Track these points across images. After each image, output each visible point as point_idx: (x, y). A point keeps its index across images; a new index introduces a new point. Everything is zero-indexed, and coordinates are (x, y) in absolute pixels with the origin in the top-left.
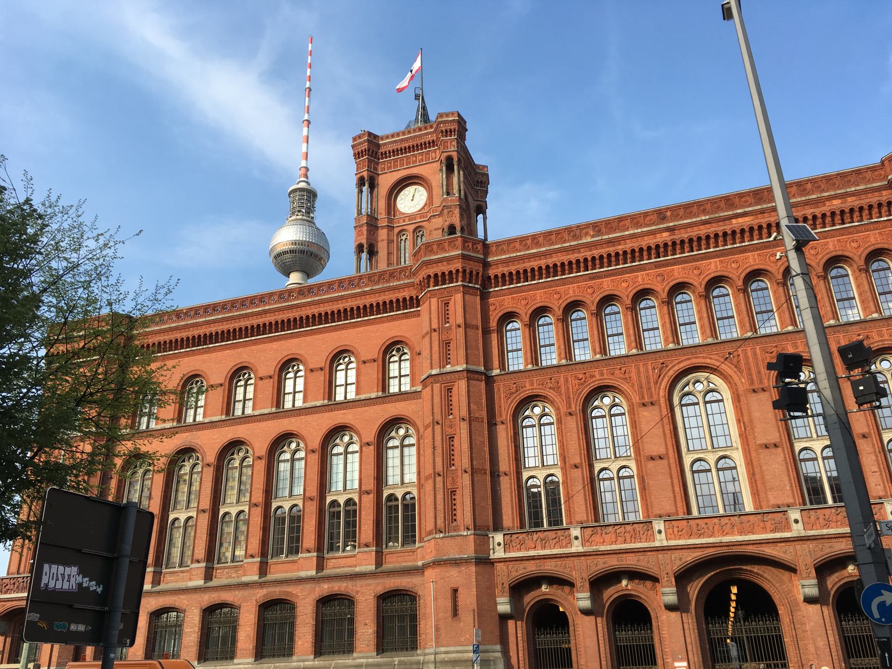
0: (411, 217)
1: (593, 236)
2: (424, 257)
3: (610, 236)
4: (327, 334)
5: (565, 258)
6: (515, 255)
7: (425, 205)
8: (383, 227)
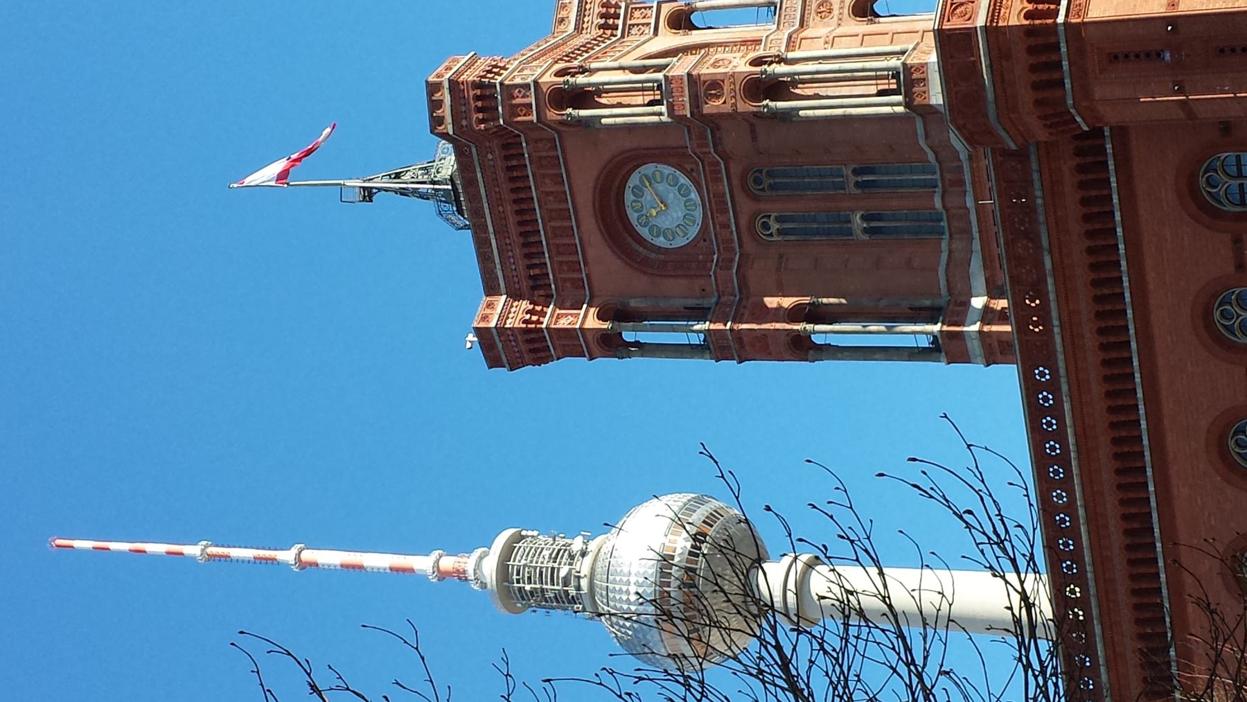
0: (714, 205)
2: (986, 116)
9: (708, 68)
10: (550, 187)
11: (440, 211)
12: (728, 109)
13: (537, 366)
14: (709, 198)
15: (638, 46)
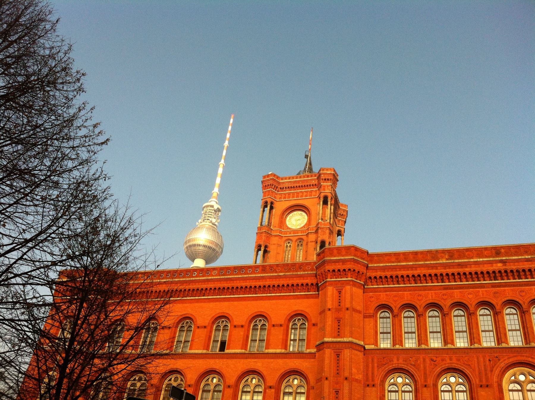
0: (295, 231)
1: (447, 259)
2: (327, 257)
3: (460, 261)
4: (249, 302)
5: (427, 272)
6: (390, 264)
7: (306, 224)
8: (276, 236)
10: (305, 194)
12: (319, 235)
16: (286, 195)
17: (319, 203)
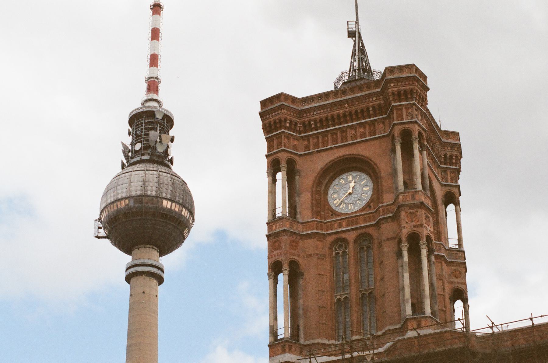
0: (351, 219)
7: (372, 200)
9: (425, 213)
11: (344, 73)
13: (262, 127)
14: (355, 216)
15: (436, 176)
16: (318, 138)
17: (393, 151)
